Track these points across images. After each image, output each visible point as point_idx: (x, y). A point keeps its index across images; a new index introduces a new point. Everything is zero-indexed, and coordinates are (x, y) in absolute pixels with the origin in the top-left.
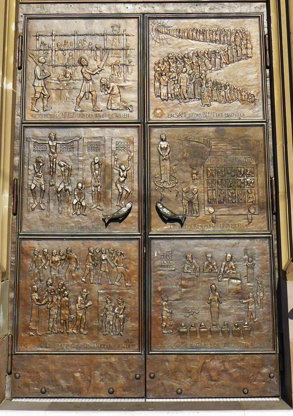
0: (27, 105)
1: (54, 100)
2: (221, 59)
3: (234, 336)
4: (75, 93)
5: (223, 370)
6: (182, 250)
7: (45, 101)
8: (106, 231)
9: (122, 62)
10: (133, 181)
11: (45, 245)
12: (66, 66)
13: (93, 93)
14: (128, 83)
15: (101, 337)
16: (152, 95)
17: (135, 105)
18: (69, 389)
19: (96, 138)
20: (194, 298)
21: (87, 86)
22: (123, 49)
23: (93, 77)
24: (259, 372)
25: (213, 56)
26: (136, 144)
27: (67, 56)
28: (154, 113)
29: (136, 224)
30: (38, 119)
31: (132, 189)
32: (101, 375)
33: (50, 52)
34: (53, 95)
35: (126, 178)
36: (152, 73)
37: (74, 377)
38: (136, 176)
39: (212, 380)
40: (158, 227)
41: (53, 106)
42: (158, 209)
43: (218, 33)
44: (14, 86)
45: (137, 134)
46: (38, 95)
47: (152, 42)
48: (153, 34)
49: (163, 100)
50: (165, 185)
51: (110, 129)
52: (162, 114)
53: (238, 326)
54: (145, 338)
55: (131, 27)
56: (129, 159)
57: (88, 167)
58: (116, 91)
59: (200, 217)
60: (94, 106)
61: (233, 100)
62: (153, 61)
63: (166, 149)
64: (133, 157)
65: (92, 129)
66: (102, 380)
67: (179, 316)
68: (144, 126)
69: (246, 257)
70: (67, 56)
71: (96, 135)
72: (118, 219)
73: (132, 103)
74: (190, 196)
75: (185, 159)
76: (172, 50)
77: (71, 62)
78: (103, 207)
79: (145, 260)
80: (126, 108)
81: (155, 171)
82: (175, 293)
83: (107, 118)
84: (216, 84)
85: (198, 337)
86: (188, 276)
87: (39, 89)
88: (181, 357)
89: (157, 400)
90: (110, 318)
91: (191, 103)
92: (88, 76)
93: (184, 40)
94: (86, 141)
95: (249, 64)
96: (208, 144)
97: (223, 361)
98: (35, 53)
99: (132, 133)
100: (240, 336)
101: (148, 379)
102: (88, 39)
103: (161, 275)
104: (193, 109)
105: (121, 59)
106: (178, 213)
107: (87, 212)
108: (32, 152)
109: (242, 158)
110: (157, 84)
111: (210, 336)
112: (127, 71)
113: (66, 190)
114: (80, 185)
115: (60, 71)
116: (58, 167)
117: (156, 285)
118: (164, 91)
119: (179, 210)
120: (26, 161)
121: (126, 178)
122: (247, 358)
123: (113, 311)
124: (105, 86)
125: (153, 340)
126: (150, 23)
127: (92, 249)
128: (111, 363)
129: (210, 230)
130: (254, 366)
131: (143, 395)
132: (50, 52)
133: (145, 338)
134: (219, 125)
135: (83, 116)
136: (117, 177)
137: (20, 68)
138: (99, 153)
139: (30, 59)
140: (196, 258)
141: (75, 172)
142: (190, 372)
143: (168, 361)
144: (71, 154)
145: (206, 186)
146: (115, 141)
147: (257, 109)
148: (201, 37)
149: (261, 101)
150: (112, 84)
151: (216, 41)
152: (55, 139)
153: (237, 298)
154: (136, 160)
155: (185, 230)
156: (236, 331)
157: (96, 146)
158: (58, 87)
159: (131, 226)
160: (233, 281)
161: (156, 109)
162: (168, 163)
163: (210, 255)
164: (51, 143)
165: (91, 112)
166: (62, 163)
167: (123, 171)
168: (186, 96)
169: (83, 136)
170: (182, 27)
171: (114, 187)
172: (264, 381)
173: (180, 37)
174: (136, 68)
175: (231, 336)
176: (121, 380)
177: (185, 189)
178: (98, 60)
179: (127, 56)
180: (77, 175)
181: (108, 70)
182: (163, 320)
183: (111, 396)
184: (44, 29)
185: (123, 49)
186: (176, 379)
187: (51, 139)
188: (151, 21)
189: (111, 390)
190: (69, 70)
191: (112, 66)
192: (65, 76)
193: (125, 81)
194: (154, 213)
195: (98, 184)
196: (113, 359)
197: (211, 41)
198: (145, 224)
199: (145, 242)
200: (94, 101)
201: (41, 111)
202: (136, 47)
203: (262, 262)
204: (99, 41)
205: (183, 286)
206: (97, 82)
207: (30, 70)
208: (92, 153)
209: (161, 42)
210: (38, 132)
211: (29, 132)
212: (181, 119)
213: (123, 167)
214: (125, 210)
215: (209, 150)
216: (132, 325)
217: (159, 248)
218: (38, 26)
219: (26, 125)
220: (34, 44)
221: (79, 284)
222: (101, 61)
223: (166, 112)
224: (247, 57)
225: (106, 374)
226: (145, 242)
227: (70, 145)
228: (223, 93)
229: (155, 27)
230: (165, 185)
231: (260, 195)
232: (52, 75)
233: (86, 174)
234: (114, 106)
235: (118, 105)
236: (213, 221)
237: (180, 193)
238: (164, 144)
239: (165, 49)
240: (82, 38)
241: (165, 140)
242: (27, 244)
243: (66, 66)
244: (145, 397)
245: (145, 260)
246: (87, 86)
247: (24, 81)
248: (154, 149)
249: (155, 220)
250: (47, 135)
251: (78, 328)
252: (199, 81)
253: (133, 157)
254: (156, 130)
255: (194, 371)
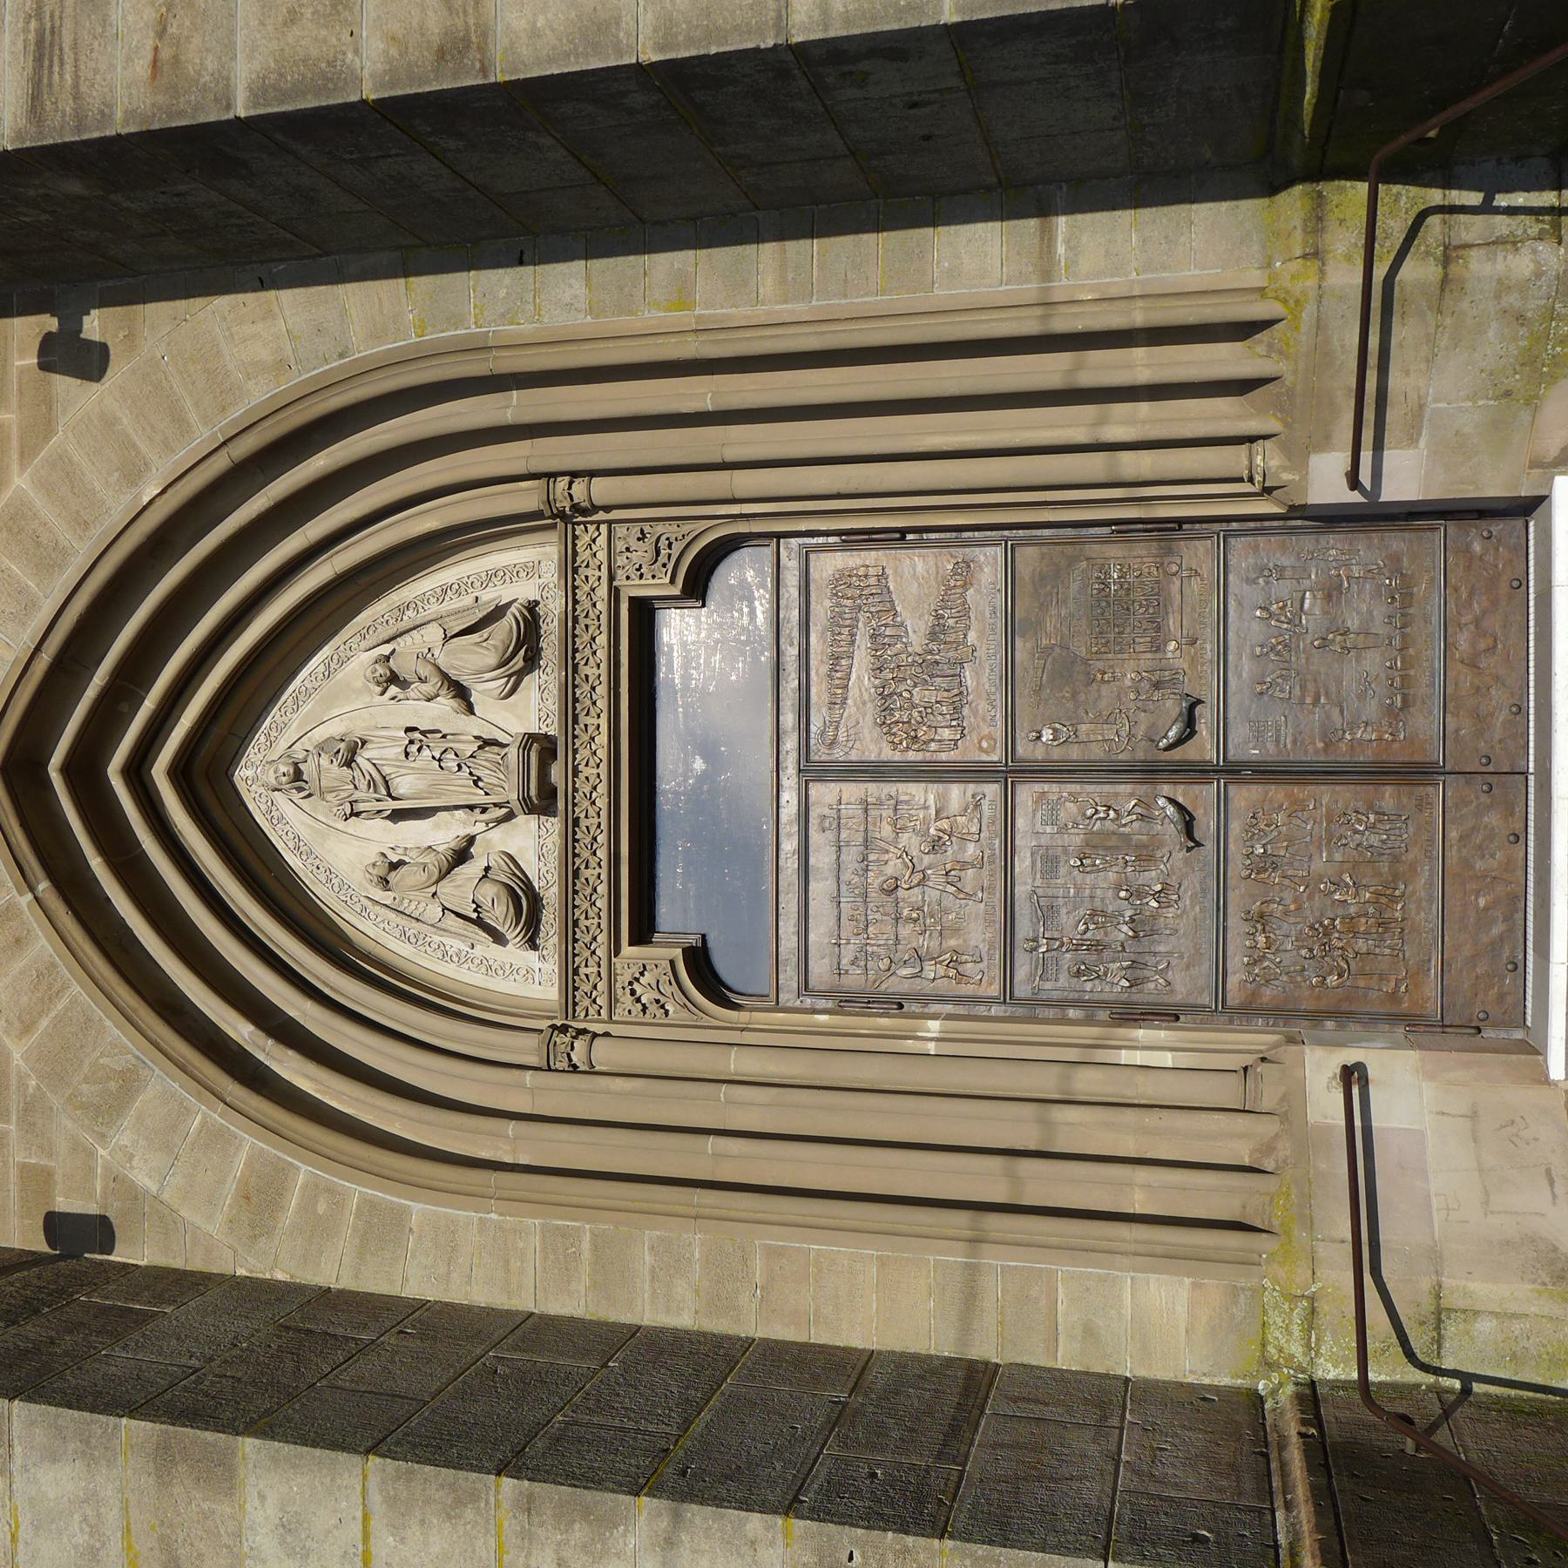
0: (970, 993)
1: (961, 941)
2: (886, 625)
3: (1410, 606)
4: (949, 901)
5: (1477, 627)
6: (1247, 702)
7: (964, 958)
8: (1210, 845)
9: (891, 812)
10: (1117, 794)
11: (1237, 961)
12: (897, 919)
13: (948, 867)
14: (931, 802)
15: (1411, 856)
16: (953, 755)
17: (971, 788)
18: (1508, 918)
19: (1033, 863)
20: (1339, 682)
21: (935, 879)
22: (866, 810)
23: (918, 868)
24: (1481, 558)
25: (880, 640)
26: (1046, 787)
27: (878, 916)
28: (987, 752)
29: (1197, 788)
30: (997, 972)
31: (1132, 795)
32: (1483, 857)
33: (870, 949)
34: (952, 943)
35: (1109, 808)
36: (912, 756)
37: (1486, 909)
38: (1107, 788)
39: (1495, 647)
40: (1204, 747)
41: (972, 943)
42: (1169, 748)
43: (837, 630)
44: (935, 1017)
45: (1027, 786)
46: (952, 973)
47: (854, 756)
48: (838, 754)
49: (963, 735)
50: (1123, 734)
51: (1018, 837)
52: (990, 737)
53: (1393, 598)
54: (1416, 773)
55: (824, 794)
56: (1072, 799)
57: (1089, 878)
58: (945, 824)
59: (1186, 667)
60: (974, 866)
61: (965, 602)
62: (888, 754)
63: (1055, 730)
64: (1070, 794)
65: (1017, 870)
66: (1493, 856)
67: (1371, 709)
68: (1012, 773)
69: (1261, 580)
70: (878, 916)
71: (1028, 862)
72: (1188, 824)
73: (969, 794)
74: (1145, 685)
75: (1074, 695)
76: (869, 718)
77: (890, 909)
78: (1165, 850)
79: (1265, 772)
80: (977, 805)
81: (1097, 752)
82: (1328, 717)
83: (997, 842)
84: (933, 635)
85: (1412, 672)
86: (1297, 691)
87: (941, 970)
88: (1450, 706)
89: (1531, 751)
90: (1374, 840)
91: (969, 683)
92: (917, 878)
93: (850, 694)
94: (1038, 883)
95: (895, 571)
96: (1046, 652)
97: (1459, 625)
98: (871, 978)
99: (1026, 794)
100: (1412, 594)
101: (1491, 768)
102: (845, 877)
103: (1294, 742)
104: (981, 679)
105: (885, 814)
106: (1177, 710)
107: (1173, 881)
108: (1059, 984)
109: (1074, 587)
110: (933, 746)
111: (1411, 651)
112: (907, 802)
113: (1132, 920)
114: (1123, 894)
115: (906, 931)
116: (1088, 935)
117: (1313, 752)
118: (946, 734)
119: (1173, 706)
120: (1076, 995)
121: (1109, 808)
122: (1452, 580)
123: (1362, 833)
124: (936, 845)
125: (1417, 758)
126: (816, 758)
127: (1245, 873)
128: (1461, 838)
129: (1209, 650)
130: (1468, 568)
131: (1522, 777)
132: (870, 949)
133: (1416, 773)
134: (1011, 630)
135: (991, 888)
136: (1108, 823)
137: (901, 1006)
138: (1063, 858)
139: (883, 987)
140: (1263, 675)
141: (1098, 904)
142: (1478, 689)
143: (1457, 731)
144: (1064, 911)
145: (1126, 656)
146: (1039, 828)
147: (982, 558)
148: (843, 662)
149: (967, 550)
150: (932, 831)
151: (853, 635)
152: (1035, 940)
153: (1339, 599)
154: (1076, 788)
155: (1210, 695)
156: (1402, 602)
157: (1049, 862)
158: (936, 934)
159: (1202, 797)
160: (1306, 606)
161: (981, 748)
162: (1083, 728)
163: (1258, 649)
164: (1044, 949)
165: (985, 872)
166: (1082, 927)
167: (1097, 812)
168: (956, 691)
169: (1029, 887)
170: (826, 697)
171: (1127, 830)
172: (1497, 549)
173: (844, 702)
174: (901, 787)
175: (1411, 611)
176: (1493, 819)
177: (1132, 696)
178: (886, 857)
179: (879, 803)
180: (1103, 900)
181: (905, 838)
182: (1380, 739)
183: (1522, 839)
184: (826, 961)
185: (866, 810)
186: (1492, 715)
187: (1035, 949)
188: (814, 757)
189: (1512, 838)
190: (906, 912)
191: (898, 830)
192: (915, 921)
193: (926, 808)
194: (1177, 754)
195: (1121, 861)
196: (1453, 834)
197: (853, 643)
198: (1199, 772)
199: (1233, 771)
200: (964, 865)
201: (981, 966)
202: (863, 786)
203: (1272, 550)
204: (851, 856)
205: (1317, 700)
206: (927, 859)
207: (905, 987)
208: (1063, 870)
209: (853, 738)
210: (1021, 973)
211: (1022, 991)
212: (999, 699)
213: (1089, 812)
214: (1170, 810)
215: (1058, 650)
216: (1388, 797)
217: (1245, 747)
218: (820, 970)
219: (1008, 995)
220: (854, 979)
221: (1310, 898)
222: (887, 852)
223: (986, 731)
224: (882, 576)
225: (1480, 847)
226: (1233, 771)
227: (1046, 912)
228: (951, 622)
229: (823, 749)
230: (1123, 734)
231: (1144, 553)
232: (914, 945)
233: (1103, 883)
234: (974, 829)
235: (971, 820)
236: (1193, 642)
237: (1140, 704)
238: (1047, 735)
239: (866, 731)
240: (844, 888)
241: (1039, 732)
242: (1234, 997)
243: (897, 919)
244: (1525, 774)
245: (1265, 772)
246: (935, 879)
247: (924, 999)
248: (1056, 754)
249: (1189, 752)
250: (1027, 956)
251: (1393, 899)
252: (928, 667)
253: (1070, 794)
254: (1020, 750)
255: (1476, 681)
